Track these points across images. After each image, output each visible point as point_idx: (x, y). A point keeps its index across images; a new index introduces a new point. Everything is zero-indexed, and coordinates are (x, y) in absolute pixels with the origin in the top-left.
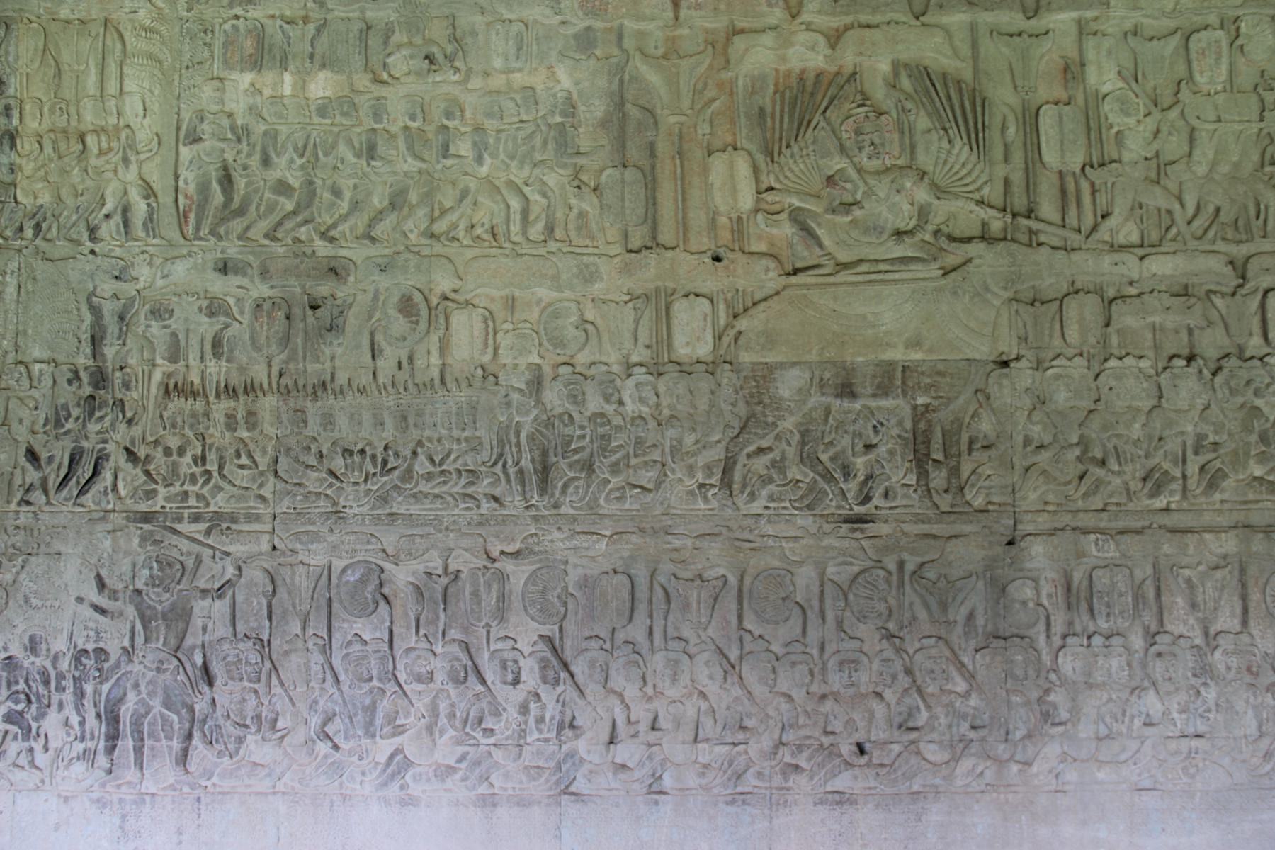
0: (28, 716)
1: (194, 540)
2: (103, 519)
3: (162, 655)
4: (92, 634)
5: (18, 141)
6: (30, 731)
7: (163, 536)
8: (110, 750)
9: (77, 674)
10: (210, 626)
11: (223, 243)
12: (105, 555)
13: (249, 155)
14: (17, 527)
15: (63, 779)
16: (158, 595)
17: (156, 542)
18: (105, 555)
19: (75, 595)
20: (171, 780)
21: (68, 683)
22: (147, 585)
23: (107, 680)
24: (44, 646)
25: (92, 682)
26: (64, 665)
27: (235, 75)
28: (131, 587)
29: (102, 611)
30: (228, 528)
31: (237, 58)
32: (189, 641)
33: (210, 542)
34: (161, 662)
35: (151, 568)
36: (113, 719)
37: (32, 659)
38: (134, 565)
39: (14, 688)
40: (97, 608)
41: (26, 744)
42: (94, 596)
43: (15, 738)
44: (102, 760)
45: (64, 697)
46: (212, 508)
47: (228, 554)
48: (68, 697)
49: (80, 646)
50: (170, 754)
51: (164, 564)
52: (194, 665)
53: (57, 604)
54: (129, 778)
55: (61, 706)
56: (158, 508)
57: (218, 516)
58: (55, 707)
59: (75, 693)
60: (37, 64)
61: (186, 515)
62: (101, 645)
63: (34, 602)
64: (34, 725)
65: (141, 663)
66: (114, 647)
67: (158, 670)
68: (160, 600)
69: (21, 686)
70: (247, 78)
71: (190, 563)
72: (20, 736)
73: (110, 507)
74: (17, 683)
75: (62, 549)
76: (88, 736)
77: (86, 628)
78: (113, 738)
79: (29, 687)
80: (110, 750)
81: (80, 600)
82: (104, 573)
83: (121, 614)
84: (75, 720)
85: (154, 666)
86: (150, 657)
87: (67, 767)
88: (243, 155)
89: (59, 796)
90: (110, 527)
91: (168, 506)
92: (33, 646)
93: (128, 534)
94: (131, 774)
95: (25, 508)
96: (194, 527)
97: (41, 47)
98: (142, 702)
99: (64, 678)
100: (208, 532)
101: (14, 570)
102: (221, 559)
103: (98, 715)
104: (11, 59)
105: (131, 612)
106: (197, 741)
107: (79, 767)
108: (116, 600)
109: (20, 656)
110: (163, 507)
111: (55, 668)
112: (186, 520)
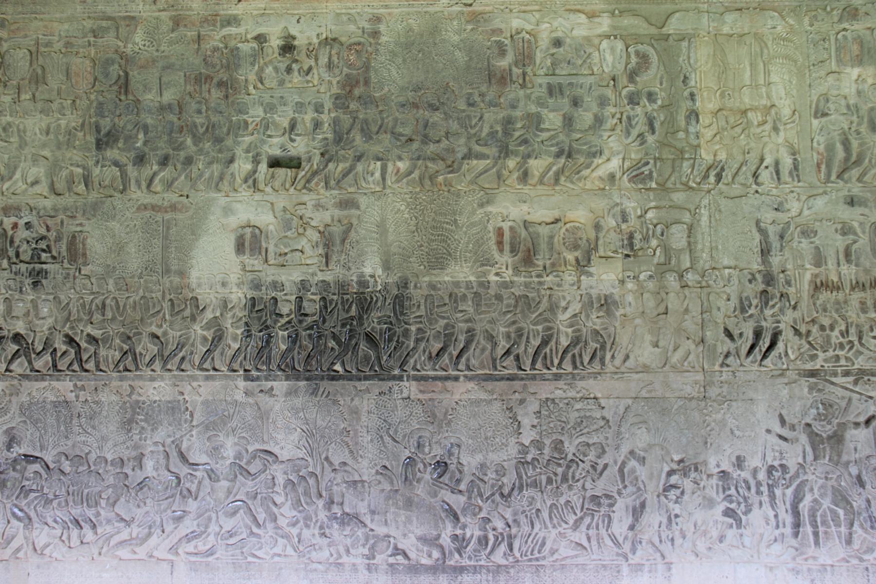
0: (739, 512)
1: (846, 389)
2: (781, 375)
3: (828, 468)
4: (777, 454)
5: (700, 117)
6: (741, 522)
7: (824, 386)
8: (796, 535)
9: (770, 482)
10: (859, 448)
11: (849, 185)
12: (784, 400)
13: (859, 124)
14: (722, 382)
15: (767, 555)
16: (823, 426)
17: (819, 390)
18: (784, 400)
19: (765, 427)
20: (842, 555)
21: (764, 489)
22: (816, 420)
23: (791, 485)
24: (746, 464)
25: (781, 487)
26: (762, 476)
27: (848, 70)
28: (803, 422)
29: (785, 439)
30: (869, 380)
31: (848, 58)
32: (845, 458)
33: (857, 389)
34: (827, 473)
35: (818, 408)
36: (796, 513)
37: (739, 472)
38: (805, 406)
39: (728, 493)
40: (781, 437)
41: (740, 531)
42: (777, 428)
43: (731, 526)
44: (794, 542)
45: (762, 499)
46: (856, 367)
47: (871, 398)
48: (765, 498)
49: (770, 463)
50: (839, 537)
51: (828, 405)
52: (850, 475)
53: (753, 434)
54: (810, 554)
55: (761, 504)
56: (818, 367)
57: (862, 372)
58: (757, 505)
59: (770, 496)
60: (709, 65)
61: (839, 372)
62: (784, 462)
63: (737, 433)
64: (743, 518)
65: (814, 474)
66: (792, 465)
67: (826, 478)
68: (824, 429)
69: (732, 491)
70: (855, 72)
71: (843, 404)
72: (734, 526)
73: (785, 367)
74: (729, 489)
75: (754, 396)
76: (781, 525)
77: (773, 450)
78: (797, 525)
79: (738, 492)
80: (796, 535)
81: (768, 431)
82: (784, 412)
83: (797, 440)
84: (771, 514)
85: (823, 476)
86: (820, 469)
87: (769, 546)
88: (854, 125)
89: (766, 566)
90: (786, 381)
91: (826, 365)
92: (740, 462)
93: (800, 385)
94: (811, 551)
95: (725, 369)
96: (844, 379)
97: (712, 53)
98: (815, 501)
99: (761, 485)
100: (856, 382)
101: (722, 411)
102: (866, 401)
103: (787, 511)
104: (692, 61)
105: (804, 439)
106: (856, 527)
107: (777, 548)
108: (795, 430)
109: (730, 470)
110: (822, 366)
111: (755, 478)
112: (840, 375)
